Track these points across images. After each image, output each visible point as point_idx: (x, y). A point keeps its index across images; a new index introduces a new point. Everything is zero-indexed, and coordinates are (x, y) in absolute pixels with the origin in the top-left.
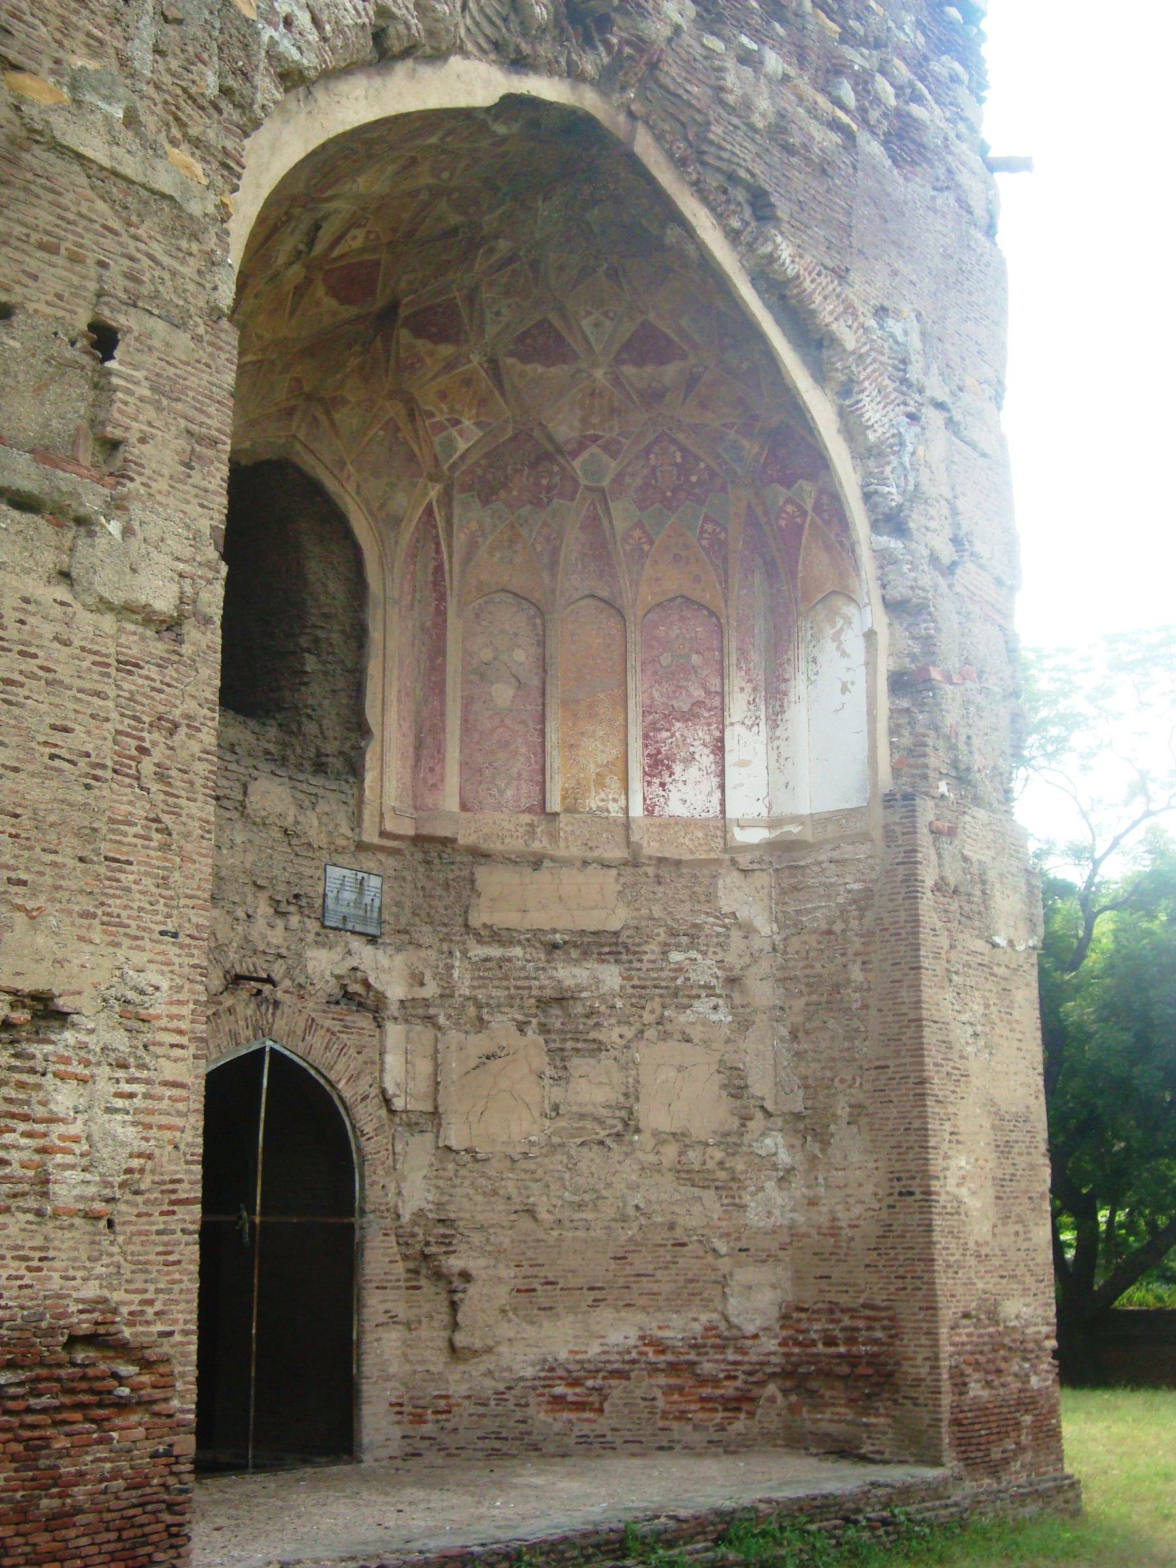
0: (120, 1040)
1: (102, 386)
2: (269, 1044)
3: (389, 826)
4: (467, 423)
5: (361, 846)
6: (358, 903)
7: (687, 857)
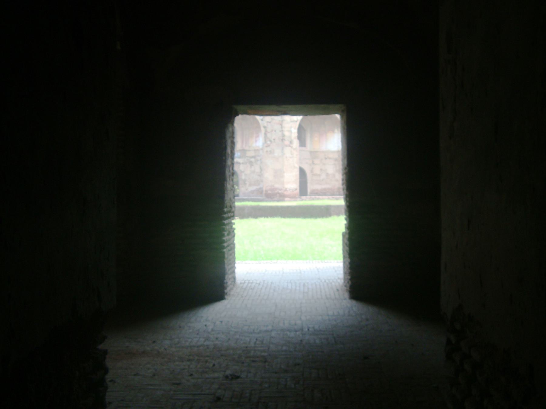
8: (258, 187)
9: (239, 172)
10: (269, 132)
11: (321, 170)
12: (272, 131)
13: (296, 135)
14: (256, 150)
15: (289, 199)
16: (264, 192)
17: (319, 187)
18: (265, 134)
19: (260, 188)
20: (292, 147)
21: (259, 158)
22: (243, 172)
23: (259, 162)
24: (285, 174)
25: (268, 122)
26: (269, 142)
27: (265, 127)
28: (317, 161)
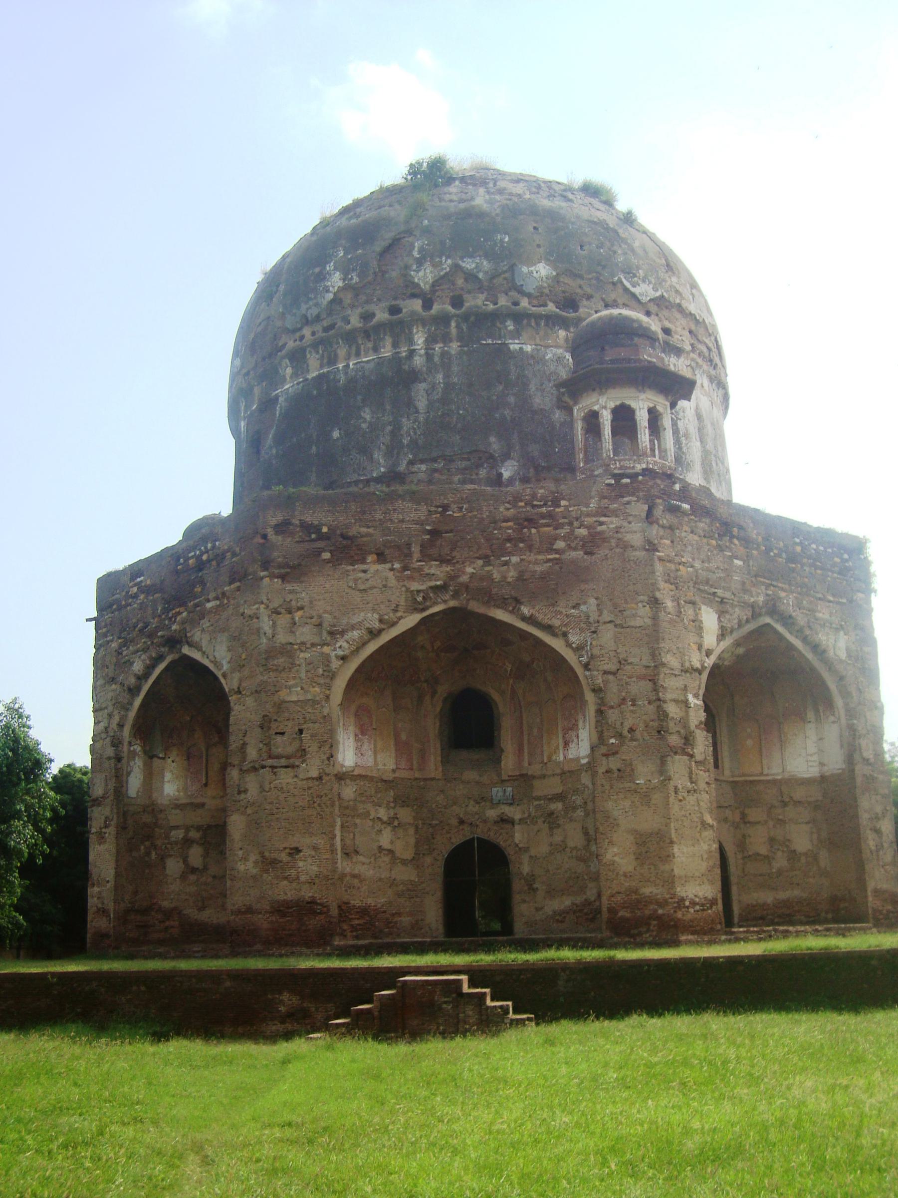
0: (313, 853)
1: (301, 740)
2: (476, 836)
3: (510, 774)
4: (507, 664)
5: (503, 781)
6: (504, 796)
7: (573, 769)
8: (579, 900)
9: (510, 852)
10: (612, 707)
11: (772, 840)
12: (624, 699)
13: (702, 716)
14: (569, 774)
15: (690, 937)
16: (605, 915)
17: (767, 897)
18: (600, 712)
19: (587, 903)
20: (692, 756)
21: (579, 802)
22: (526, 850)
23: (580, 813)
24: (676, 849)
25: (606, 672)
26: (613, 741)
27: (596, 691)
28: (755, 814)
